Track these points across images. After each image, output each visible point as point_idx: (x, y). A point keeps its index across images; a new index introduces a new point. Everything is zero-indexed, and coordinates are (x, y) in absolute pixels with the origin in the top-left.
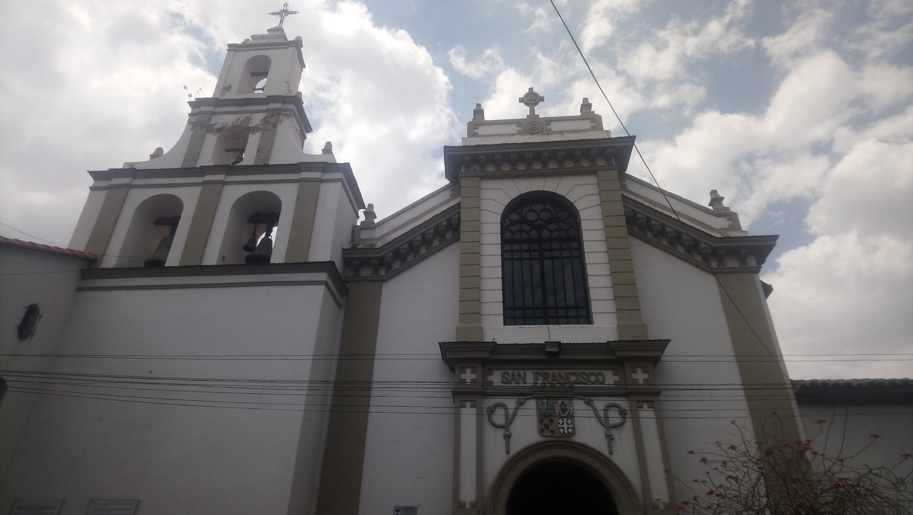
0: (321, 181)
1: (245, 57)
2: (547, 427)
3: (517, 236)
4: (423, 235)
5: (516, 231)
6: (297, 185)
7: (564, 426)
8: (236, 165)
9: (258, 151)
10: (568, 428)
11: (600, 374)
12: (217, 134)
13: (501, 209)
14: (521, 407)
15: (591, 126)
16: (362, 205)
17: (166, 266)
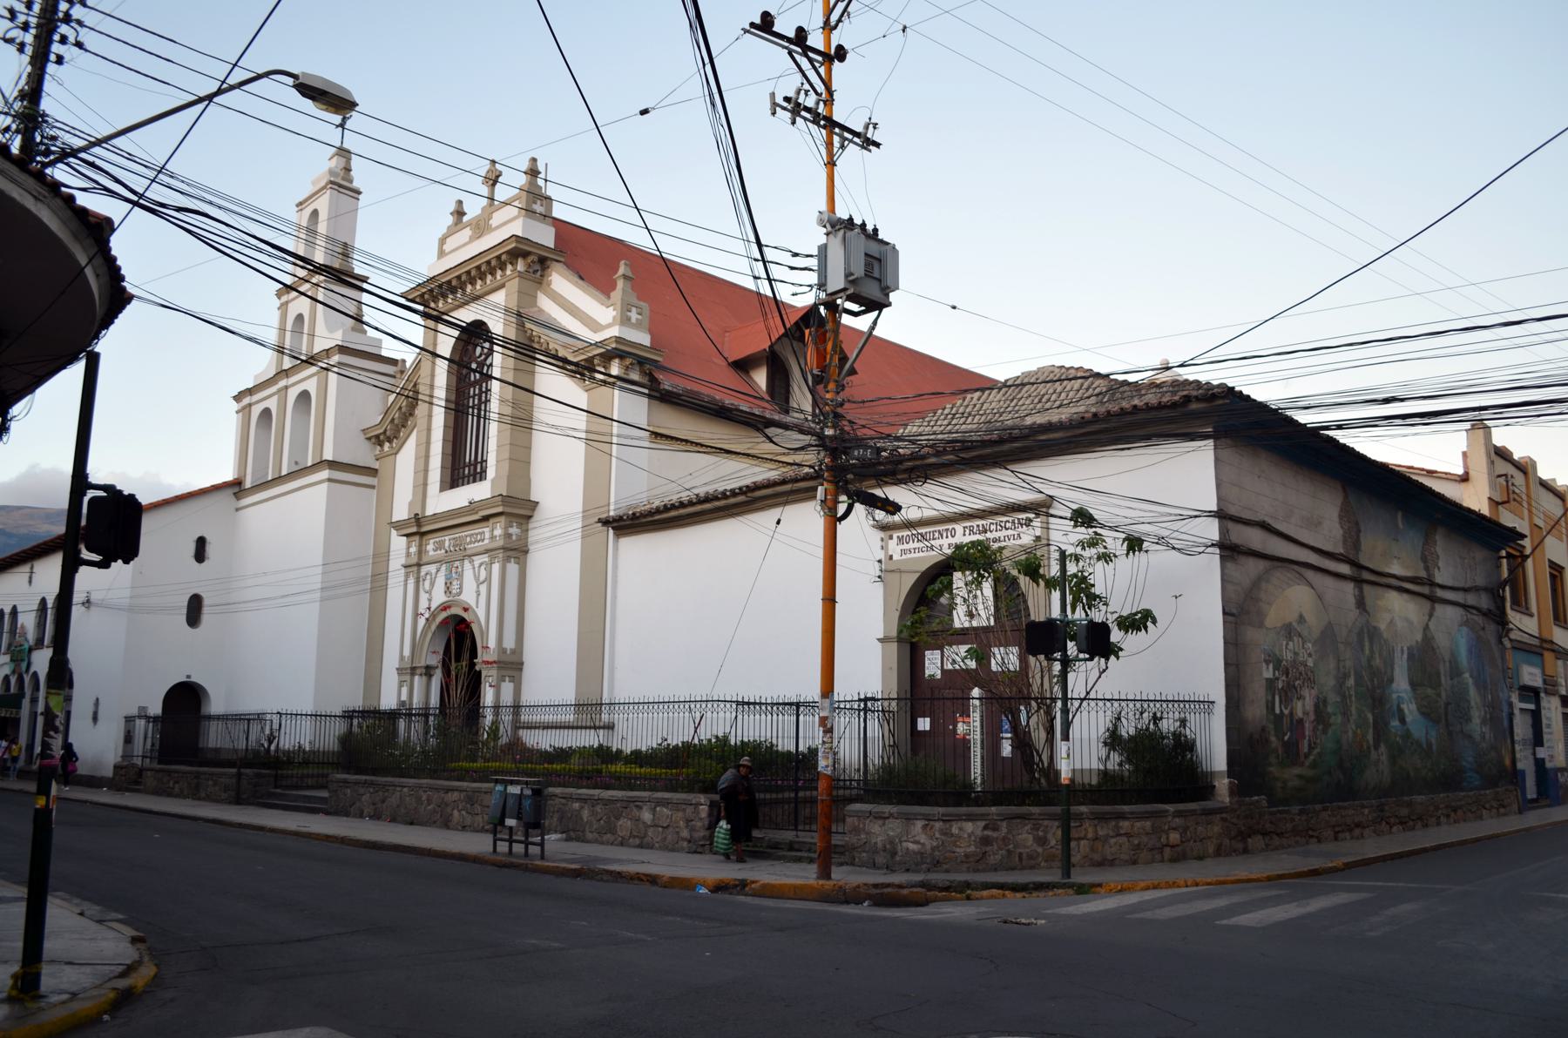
2: (448, 588)
7: (455, 587)
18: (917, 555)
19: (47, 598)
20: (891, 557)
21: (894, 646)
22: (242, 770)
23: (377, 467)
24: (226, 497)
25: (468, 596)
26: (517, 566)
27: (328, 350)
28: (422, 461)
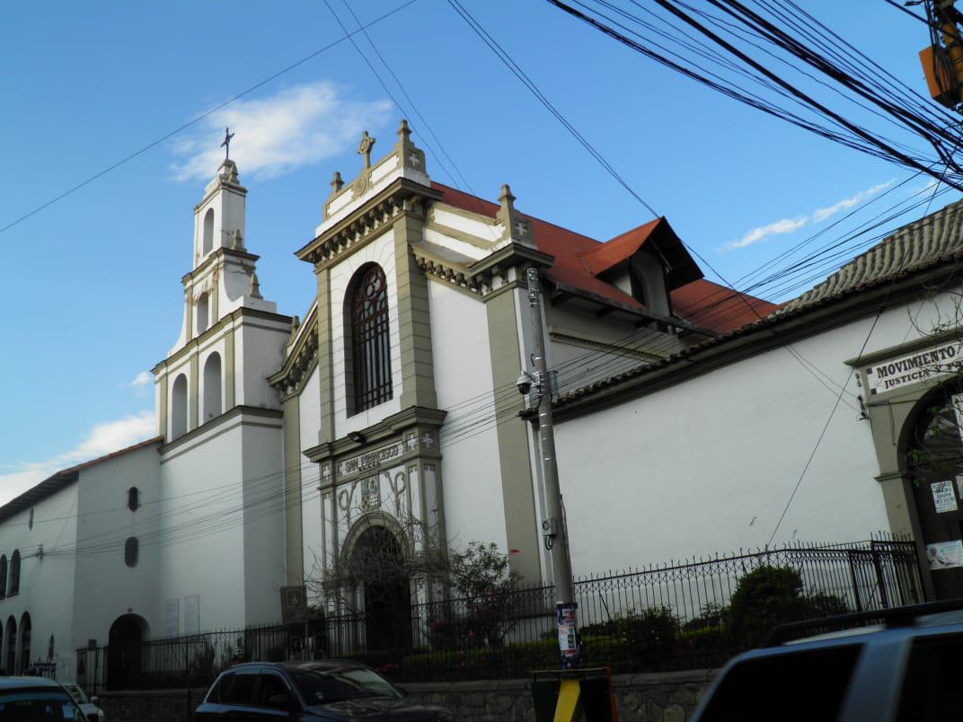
0: (233, 330)
2: (366, 502)
4: (306, 343)
6: (223, 340)
7: (373, 500)
16: (287, 320)
18: (907, 383)
19: (7, 556)
20: (874, 391)
21: (898, 484)
22: (192, 690)
23: (282, 409)
24: (152, 452)
25: (388, 506)
26: (432, 473)
28: (328, 394)
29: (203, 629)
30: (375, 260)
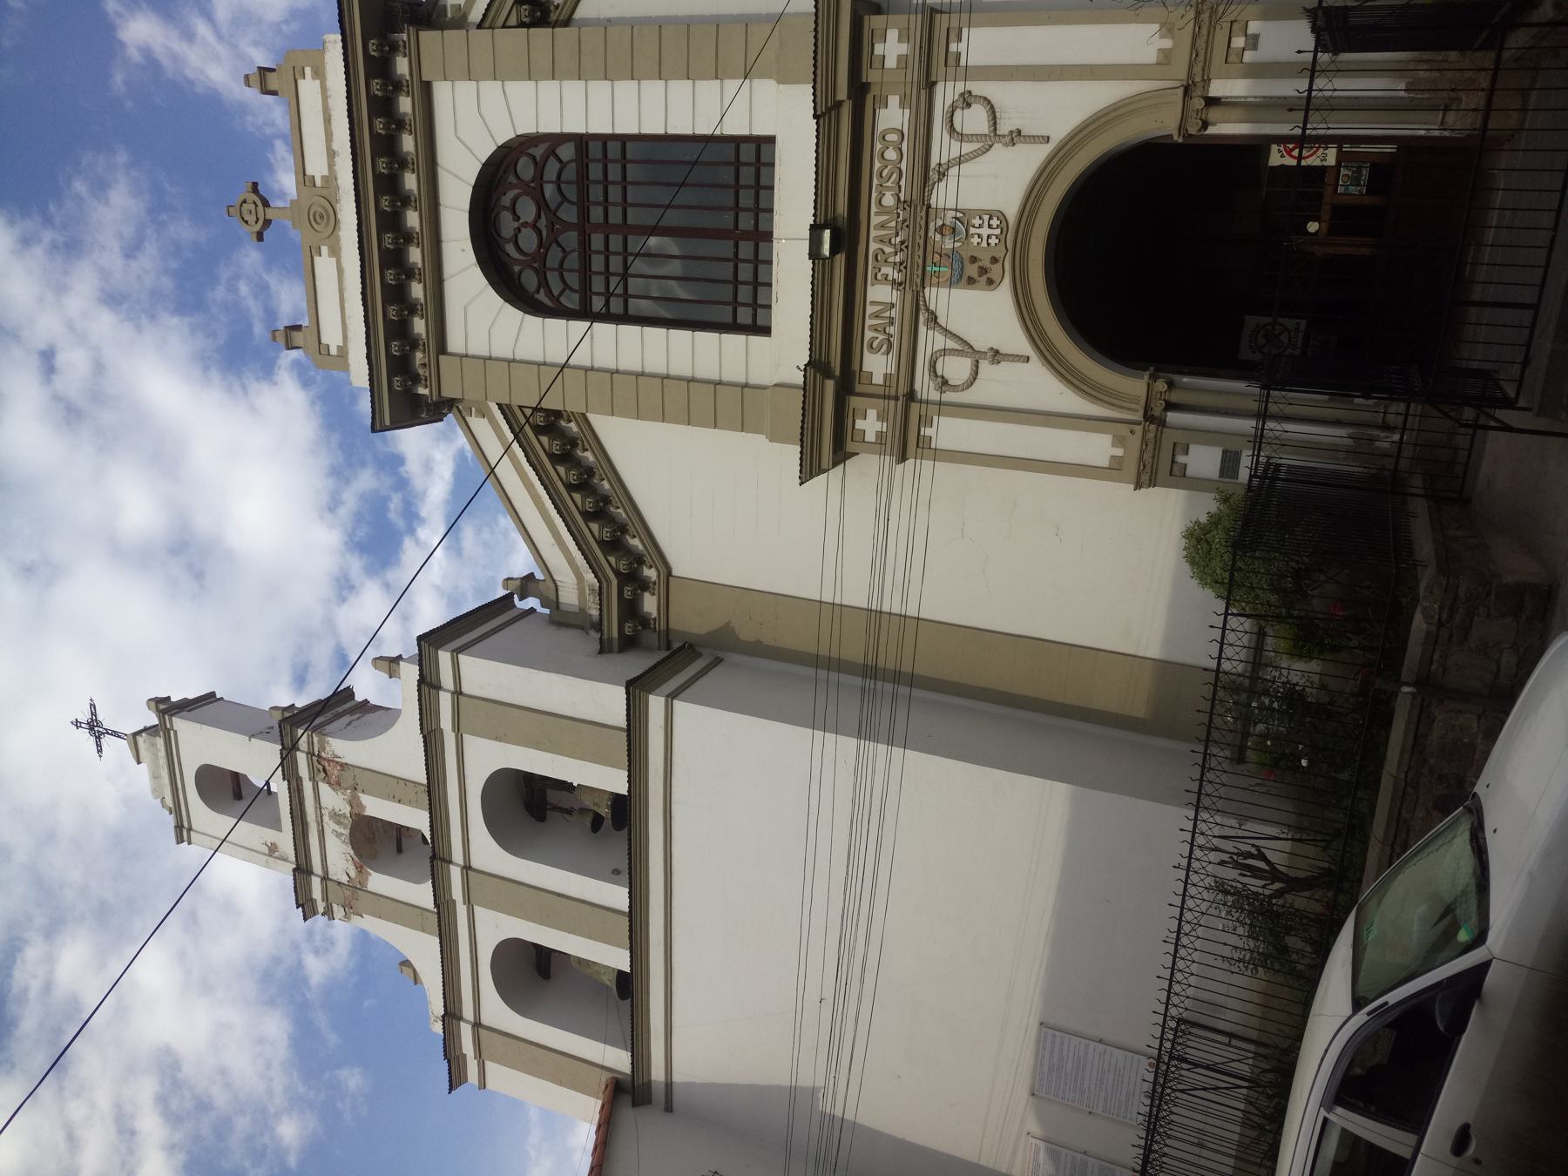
0: (458, 693)
1: (199, 812)
2: (983, 271)
3: (573, 280)
4: (570, 488)
5: (564, 281)
7: (984, 236)
8: (429, 841)
9: (399, 801)
10: (990, 226)
11: (884, 137)
12: (367, 871)
13: (512, 314)
14: (941, 321)
15: (313, 78)
16: (505, 603)
17: (628, 970)
23: (681, 644)
27: (421, 675)
29: (1144, 1033)
30: (471, 172)
